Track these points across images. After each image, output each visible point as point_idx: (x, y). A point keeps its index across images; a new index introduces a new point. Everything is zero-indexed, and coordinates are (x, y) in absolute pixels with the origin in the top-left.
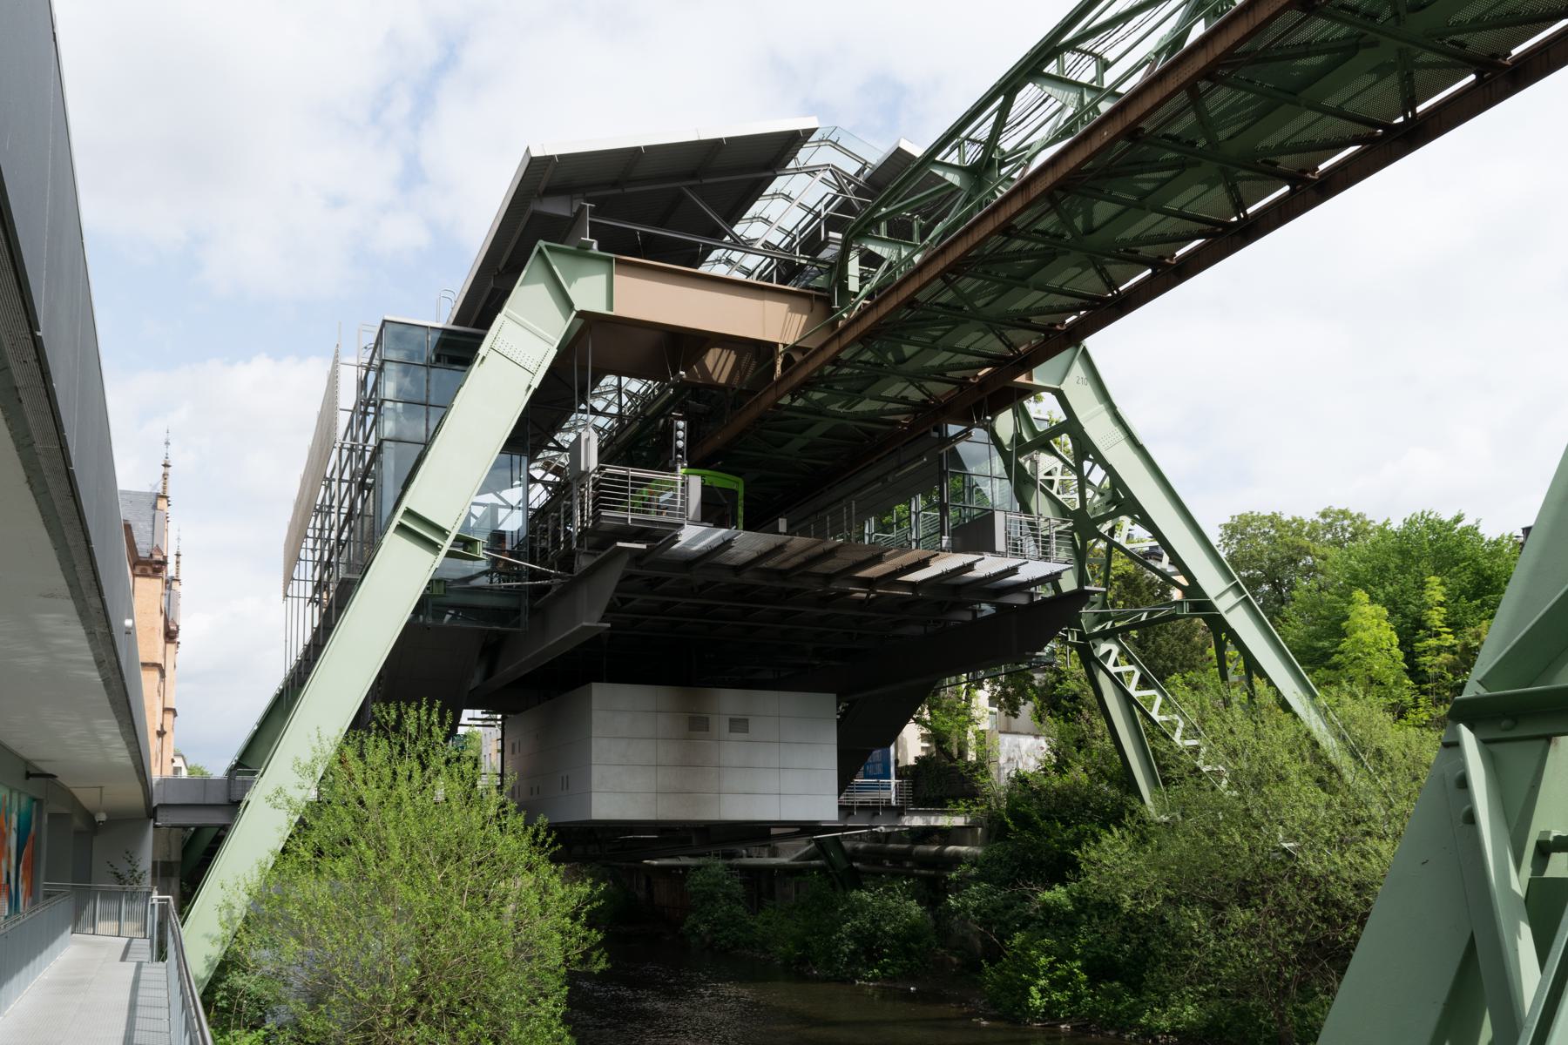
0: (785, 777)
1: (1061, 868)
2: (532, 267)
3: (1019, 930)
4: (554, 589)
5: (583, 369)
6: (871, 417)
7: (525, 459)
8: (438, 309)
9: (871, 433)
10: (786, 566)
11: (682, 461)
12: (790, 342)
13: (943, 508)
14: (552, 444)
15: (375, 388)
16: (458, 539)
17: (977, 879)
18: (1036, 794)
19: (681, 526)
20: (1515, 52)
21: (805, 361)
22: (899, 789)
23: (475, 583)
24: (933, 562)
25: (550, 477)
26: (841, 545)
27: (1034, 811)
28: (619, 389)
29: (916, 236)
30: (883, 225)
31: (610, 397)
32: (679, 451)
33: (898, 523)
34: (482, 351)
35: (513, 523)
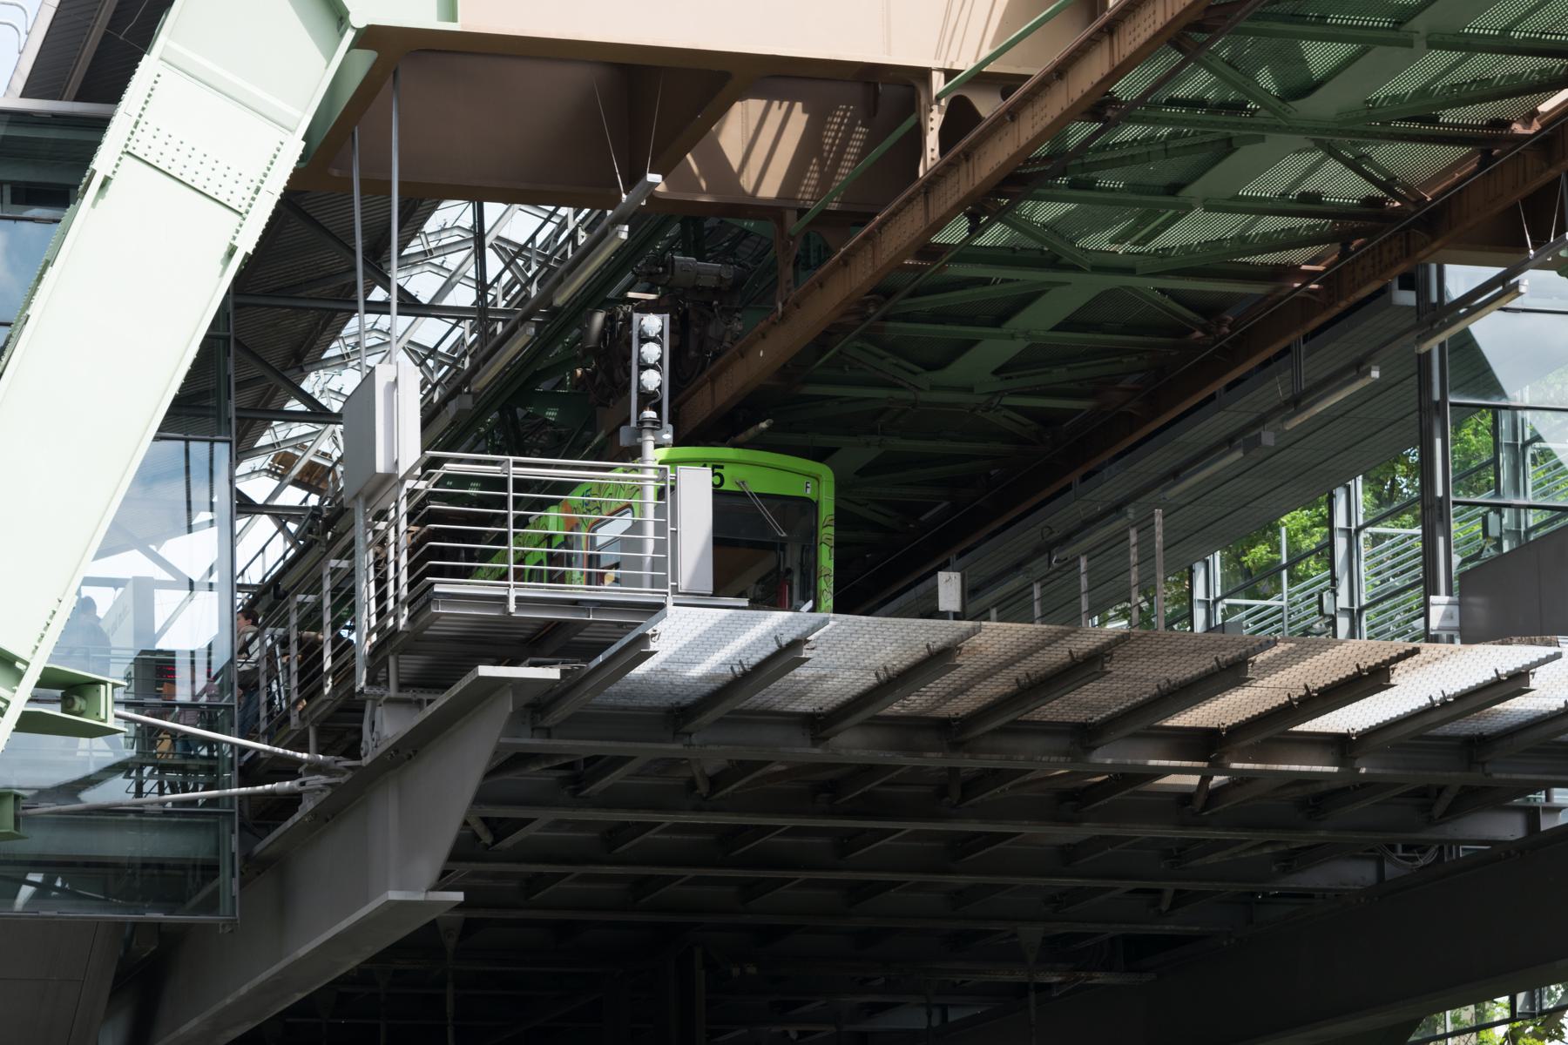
6: (1210, 262)
7: (222, 450)
9: (1210, 309)
11: (657, 425)
12: (965, 63)
13: (1433, 515)
14: (295, 405)
16: (49, 679)
19: (657, 608)
21: (1012, 114)
23: (92, 797)
24: (1401, 675)
25: (293, 496)
26: (1122, 639)
28: (478, 234)
31: (453, 261)
32: (648, 399)
33: (1291, 565)
35: (196, 628)
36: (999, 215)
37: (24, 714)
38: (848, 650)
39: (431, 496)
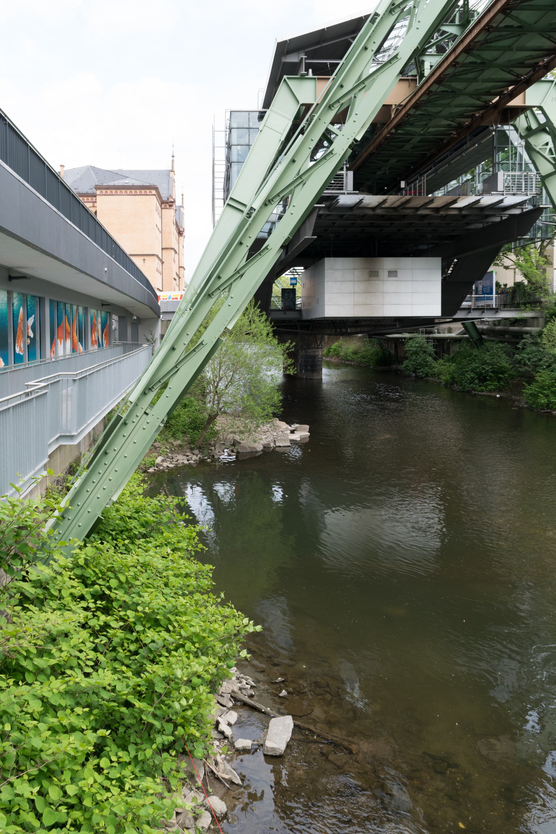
9: (442, 140)
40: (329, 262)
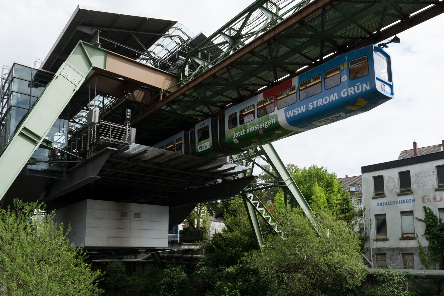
0: (153, 233)
1: (231, 262)
2: (76, 49)
3: (218, 281)
4: (78, 164)
5: (93, 90)
6: (189, 117)
8: (37, 59)
10: (162, 162)
11: (129, 123)
12: (165, 89)
15: (8, 89)
17: (205, 265)
18: (223, 239)
20: (412, 15)
21: (169, 96)
22: (181, 237)
27: (222, 243)
29: (209, 59)
30: (200, 54)
32: (128, 119)
34: (57, 74)
36: (170, 106)
37: (41, 145)
38: (152, 151)
39: (100, 126)
40: (90, 203)
